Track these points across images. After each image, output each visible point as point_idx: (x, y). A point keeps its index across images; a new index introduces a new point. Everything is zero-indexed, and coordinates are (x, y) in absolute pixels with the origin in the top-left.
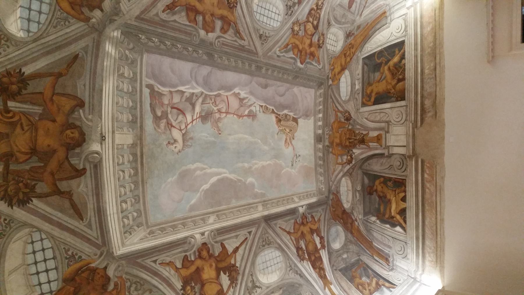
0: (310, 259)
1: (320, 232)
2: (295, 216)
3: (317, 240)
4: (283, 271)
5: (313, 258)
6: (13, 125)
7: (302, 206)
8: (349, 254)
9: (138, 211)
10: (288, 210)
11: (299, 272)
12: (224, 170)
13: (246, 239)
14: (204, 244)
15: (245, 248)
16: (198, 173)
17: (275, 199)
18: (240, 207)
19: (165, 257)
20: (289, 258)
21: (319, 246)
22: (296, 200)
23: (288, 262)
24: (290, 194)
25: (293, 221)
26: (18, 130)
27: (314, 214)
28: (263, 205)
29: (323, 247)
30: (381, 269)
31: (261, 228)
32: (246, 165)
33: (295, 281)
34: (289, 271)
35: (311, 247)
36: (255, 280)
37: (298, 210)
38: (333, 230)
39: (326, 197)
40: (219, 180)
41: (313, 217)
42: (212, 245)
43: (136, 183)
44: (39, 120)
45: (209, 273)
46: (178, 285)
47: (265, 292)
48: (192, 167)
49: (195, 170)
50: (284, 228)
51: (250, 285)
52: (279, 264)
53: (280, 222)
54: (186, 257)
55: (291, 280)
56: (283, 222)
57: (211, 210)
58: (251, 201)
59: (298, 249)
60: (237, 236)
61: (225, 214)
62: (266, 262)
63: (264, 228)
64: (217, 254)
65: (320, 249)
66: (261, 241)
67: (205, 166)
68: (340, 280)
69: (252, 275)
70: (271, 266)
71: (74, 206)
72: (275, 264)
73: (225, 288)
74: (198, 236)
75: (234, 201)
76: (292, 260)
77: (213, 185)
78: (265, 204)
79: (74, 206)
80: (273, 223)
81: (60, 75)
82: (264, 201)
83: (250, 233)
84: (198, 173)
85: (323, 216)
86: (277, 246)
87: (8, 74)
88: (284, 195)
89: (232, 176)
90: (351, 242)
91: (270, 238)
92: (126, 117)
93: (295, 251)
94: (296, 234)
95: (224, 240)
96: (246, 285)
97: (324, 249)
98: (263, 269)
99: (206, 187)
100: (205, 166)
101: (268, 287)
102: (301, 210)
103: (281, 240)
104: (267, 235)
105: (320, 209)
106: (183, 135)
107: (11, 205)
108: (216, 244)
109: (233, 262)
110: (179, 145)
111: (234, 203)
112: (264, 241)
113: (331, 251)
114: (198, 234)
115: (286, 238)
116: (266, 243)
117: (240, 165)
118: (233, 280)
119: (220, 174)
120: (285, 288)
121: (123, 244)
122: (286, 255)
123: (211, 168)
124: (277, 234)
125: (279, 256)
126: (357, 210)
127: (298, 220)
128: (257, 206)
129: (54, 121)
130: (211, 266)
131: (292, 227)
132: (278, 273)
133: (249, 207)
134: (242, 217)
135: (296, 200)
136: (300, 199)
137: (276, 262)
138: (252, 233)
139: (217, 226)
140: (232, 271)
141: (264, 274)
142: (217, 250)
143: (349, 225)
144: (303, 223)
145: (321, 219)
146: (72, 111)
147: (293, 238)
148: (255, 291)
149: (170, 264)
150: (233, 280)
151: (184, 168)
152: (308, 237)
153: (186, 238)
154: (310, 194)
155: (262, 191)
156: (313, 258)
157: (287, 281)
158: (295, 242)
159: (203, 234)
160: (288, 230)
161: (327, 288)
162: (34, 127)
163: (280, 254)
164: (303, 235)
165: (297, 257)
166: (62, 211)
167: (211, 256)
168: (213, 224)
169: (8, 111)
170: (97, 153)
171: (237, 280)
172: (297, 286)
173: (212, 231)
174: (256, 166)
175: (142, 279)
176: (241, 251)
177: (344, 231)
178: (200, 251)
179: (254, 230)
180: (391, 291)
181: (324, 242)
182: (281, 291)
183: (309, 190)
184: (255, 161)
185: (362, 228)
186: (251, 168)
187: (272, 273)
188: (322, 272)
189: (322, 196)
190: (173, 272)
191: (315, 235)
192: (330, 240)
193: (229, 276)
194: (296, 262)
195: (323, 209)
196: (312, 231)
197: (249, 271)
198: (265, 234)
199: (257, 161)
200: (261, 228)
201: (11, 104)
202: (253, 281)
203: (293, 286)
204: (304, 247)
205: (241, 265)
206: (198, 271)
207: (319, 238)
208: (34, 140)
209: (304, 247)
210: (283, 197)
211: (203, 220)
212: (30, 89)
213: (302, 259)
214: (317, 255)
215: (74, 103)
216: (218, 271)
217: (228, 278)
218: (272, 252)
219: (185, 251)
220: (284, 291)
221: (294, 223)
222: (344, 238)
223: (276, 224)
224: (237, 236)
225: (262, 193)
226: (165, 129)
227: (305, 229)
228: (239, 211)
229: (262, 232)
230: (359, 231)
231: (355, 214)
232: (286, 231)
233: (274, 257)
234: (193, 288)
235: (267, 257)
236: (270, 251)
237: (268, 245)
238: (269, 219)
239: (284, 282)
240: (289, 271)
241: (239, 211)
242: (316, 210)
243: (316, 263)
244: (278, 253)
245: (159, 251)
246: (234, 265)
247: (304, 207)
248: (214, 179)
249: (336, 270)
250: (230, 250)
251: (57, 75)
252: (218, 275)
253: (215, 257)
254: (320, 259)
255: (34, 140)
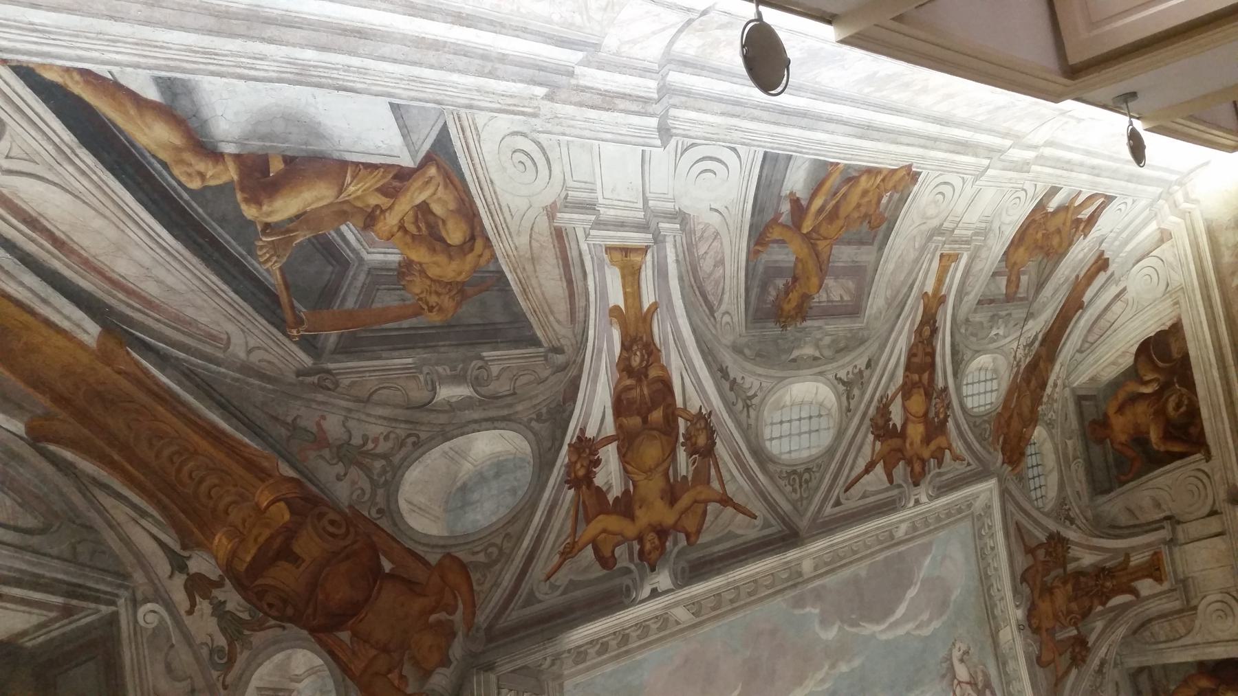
0: (671, 415)
1: (576, 503)
2: (694, 555)
3: (610, 473)
4: (772, 399)
5: (657, 415)
6: (1069, 612)
7: (655, 593)
8: (418, 394)
9: (981, 537)
10: (719, 572)
11: (727, 385)
12: (884, 637)
13: (846, 491)
14: (916, 484)
15: (852, 469)
16: (925, 617)
17: (761, 599)
18: (851, 562)
19: (961, 468)
20: (745, 430)
21: (610, 455)
22: (681, 614)
23: (752, 421)
24: (707, 628)
25: (704, 539)
26: (1064, 609)
27: (598, 572)
28: (800, 574)
29: (586, 449)
30: (87, 242)
31: (809, 514)
32: (844, 668)
33: (748, 366)
34: (755, 395)
35: (651, 452)
36: (844, 398)
37: (675, 576)
38: (486, 512)
39: (490, 668)
40: (889, 611)
41: (606, 561)
42: (906, 481)
43: (988, 577)
44: (1054, 628)
45: (916, 432)
46: (950, 424)
47: (829, 367)
48: (936, 624)
49: (930, 620)
50: (741, 516)
51: (856, 392)
52: (777, 419)
53: (748, 531)
54: (940, 464)
55: (760, 370)
56: (740, 532)
57: (902, 548)
58: (828, 580)
59: (707, 452)
60: (864, 496)
61: (881, 542)
62: (810, 432)
63: (802, 516)
64: (901, 463)
65: (608, 440)
66: (813, 484)
67: (917, 632)
68: (562, 308)
69: (849, 410)
70: (800, 419)
71: (1022, 538)
72: (790, 421)
73: (899, 399)
74: (924, 499)
75: (863, 573)
76: (739, 424)
77: (899, 600)
78: (795, 578)
79: (1022, 538)
80: (776, 528)
81: (1056, 685)
82: (795, 586)
83: (838, 503)
84: (925, 617)
85: (539, 569)
86: (771, 467)
87: (1084, 661)
88: (732, 618)
89: (869, 629)
90: (351, 454)
91: (789, 488)
92: (1011, 665)
93: (720, 449)
94: (703, 497)
95: (887, 490)
96: (863, 394)
97: (581, 439)
98: (820, 416)
99: (912, 592)
100: (917, 632)
101: (821, 373)
102: (663, 579)
103: (752, 480)
104: (796, 496)
105: (549, 599)
106: (954, 677)
107: (1058, 533)
108: (901, 482)
109: (878, 444)
110: (956, 654)
111: (861, 569)
112: (807, 482)
113: (543, 428)
114: (925, 503)
115: (740, 487)
116: (800, 476)
117: (857, 663)
118: (884, 410)
119: (891, 627)
120: (784, 357)
121: (985, 491)
122: (752, 438)
123: (908, 633)
124: (766, 499)
125: (772, 439)
126: (183, 657)
127: (683, 542)
128: (816, 568)
129: (1047, 630)
130: (911, 444)
131: (709, 518)
132: (787, 399)
133: (832, 564)
134: (850, 539)
135: (681, 614)
136: (663, 620)
137: (786, 426)
138: (832, 502)
139: (895, 517)
140: (882, 429)
141: (821, 405)
142: (900, 470)
143: (309, 546)
144: (662, 533)
145: (556, 559)
146: (1041, 650)
147: (715, 485)
148: (851, 376)
149: (956, 458)
150: (884, 410)
151: (945, 618)
152: (652, 487)
153: (937, 497)
154: (604, 648)
155: (802, 612)
156: (657, 415)
157: (772, 372)
158: (713, 472)
159: (917, 502)
160: (730, 510)
161: (646, 306)
162: (1056, 617)
163: (768, 444)
164: (671, 494)
165: (717, 427)
166: (1029, 531)
167: (909, 462)
168: (899, 521)
169: (1075, 624)
170: (1017, 606)
171: (878, 408)
172: (747, 351)
173: (904, 507)
174: (820, 675)
175: (980, 443)
176: (861, 464)
177: (390, 510)
178: (923, 473)
179: (828, 510)
180: (166, 85)
181: (570, 466)
182: (795, 354)
183: (609, 668)
184: (826, 686)
185: (144, 534)
186: (833, 666)
187: (802, 404)
188: (636, 361)
189: (531, 660)
190: (954, 445)
191: (616, 491)
192: (526, 475)
193: (890, 419)
194: (726, 416)
195: (531, 599)
196: (626, 506)
197: (851, 419)
198: (802, 498)
199: (820, 689)
200: (809, 514)
201: (1075, 632)
202: (848, 398)
203: (759, 355)
204: (682, 454)
205: (866, 436)
206: (927, 440)
207: (599, 481)
208: (1052, 601)
209: (682, 454)
210: (734, 610)
211: (914, 528)
212: (1068, 655)
213: (703, 422)
214: (635, 421)
215: (1043, 659)
216: (903, 435)
217: (892, 416)
218: (790, 452)
219: (940, 475)
220: (791, 350)
221: (699, 532)
222: (414, 475)
223: (767, 525)
224: (864, 496)
225: (803, 607)
226: (976, 672)
227: (657, 512)
228: (855, 553)
229: (810, 503)
230: (189, 517)
231: (204, 625)
232: (739, 508)
233: (785, 441)
234: (937, 414)
235: (805, 444)
236: (794, 455)
237: (794, 472)
238: (783, 539)
239: (780, 374)
240: (755, 395)
241: (855, 553)
242: (578, 594)
243: (645, 393)
244: (774, 448)
245: (964, 479)
246: (877, 437)
247: (646, 592)
248: (900, 611)
249: (558, 350)
250: (879, 468)
251: (1059, 681)
252: (904, 426)
253: (903, 459)
254: (620, 406)
255: (1052, 601)
